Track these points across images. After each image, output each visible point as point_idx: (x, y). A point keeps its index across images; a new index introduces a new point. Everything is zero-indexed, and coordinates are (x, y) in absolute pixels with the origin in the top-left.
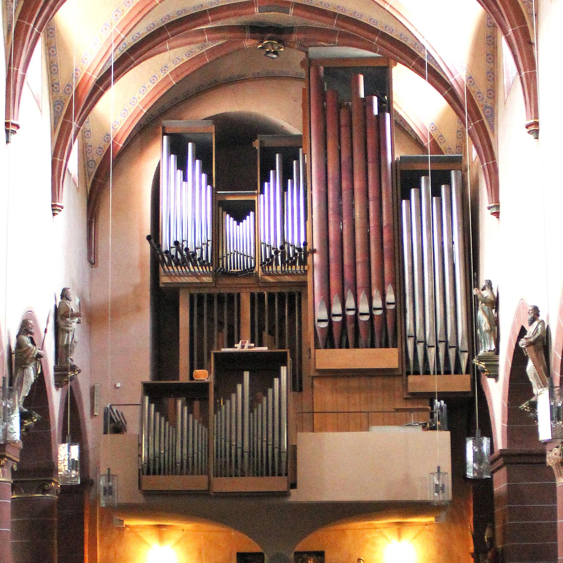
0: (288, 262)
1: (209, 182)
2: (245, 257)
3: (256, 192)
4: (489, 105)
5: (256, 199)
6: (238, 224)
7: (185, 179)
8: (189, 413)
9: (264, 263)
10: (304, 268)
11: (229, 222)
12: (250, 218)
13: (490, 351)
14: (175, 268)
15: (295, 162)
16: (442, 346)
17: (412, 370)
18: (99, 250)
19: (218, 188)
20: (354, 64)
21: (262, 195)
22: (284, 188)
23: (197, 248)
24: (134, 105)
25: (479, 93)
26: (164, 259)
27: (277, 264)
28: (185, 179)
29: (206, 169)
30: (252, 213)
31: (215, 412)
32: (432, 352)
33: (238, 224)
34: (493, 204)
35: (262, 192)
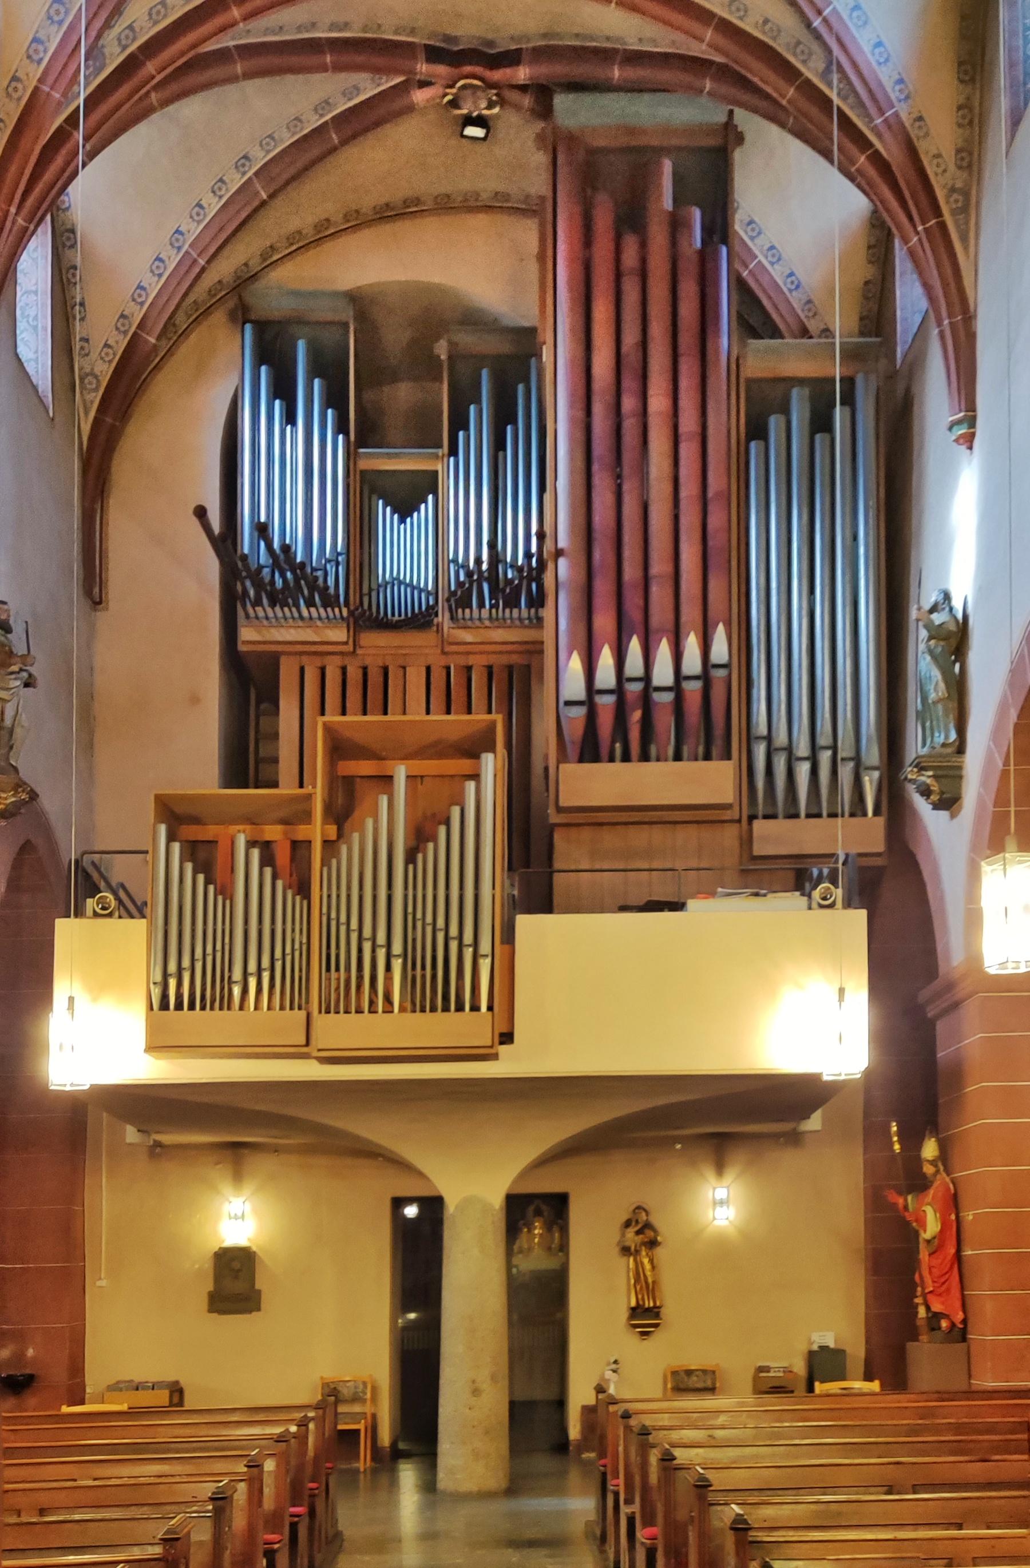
0: (503, 590)
1: (342, 427)
2: (416, 592)
3: (440, 452)
4: (959, 185)
5: (439, 468)
6: (402, 521)
7: (290, 418)
8: (262, 865)
9: (454, 593)
10: (537, 612)
11: (384, 515)
12: (426, 510)
13: (944, 745)
14: (269, 610)
15: (521, 388)
16: (825, 758)
17: (761, 809)
18: (111, 565)
19: (363, 441)
20: (655, 142)
21: (452, 459)
22: (499, 444)
23: (317, 570)
24: (179, 248)
25: (938, 156)
26: (245, 592)
27: (481, 605)
28: (290, 418)
29: (335, 399)
30: (430, 497)
31: (325, 862)
32: (803, 770)
33: (402, 521)
34: (962, 414)
35: (453, 451)
